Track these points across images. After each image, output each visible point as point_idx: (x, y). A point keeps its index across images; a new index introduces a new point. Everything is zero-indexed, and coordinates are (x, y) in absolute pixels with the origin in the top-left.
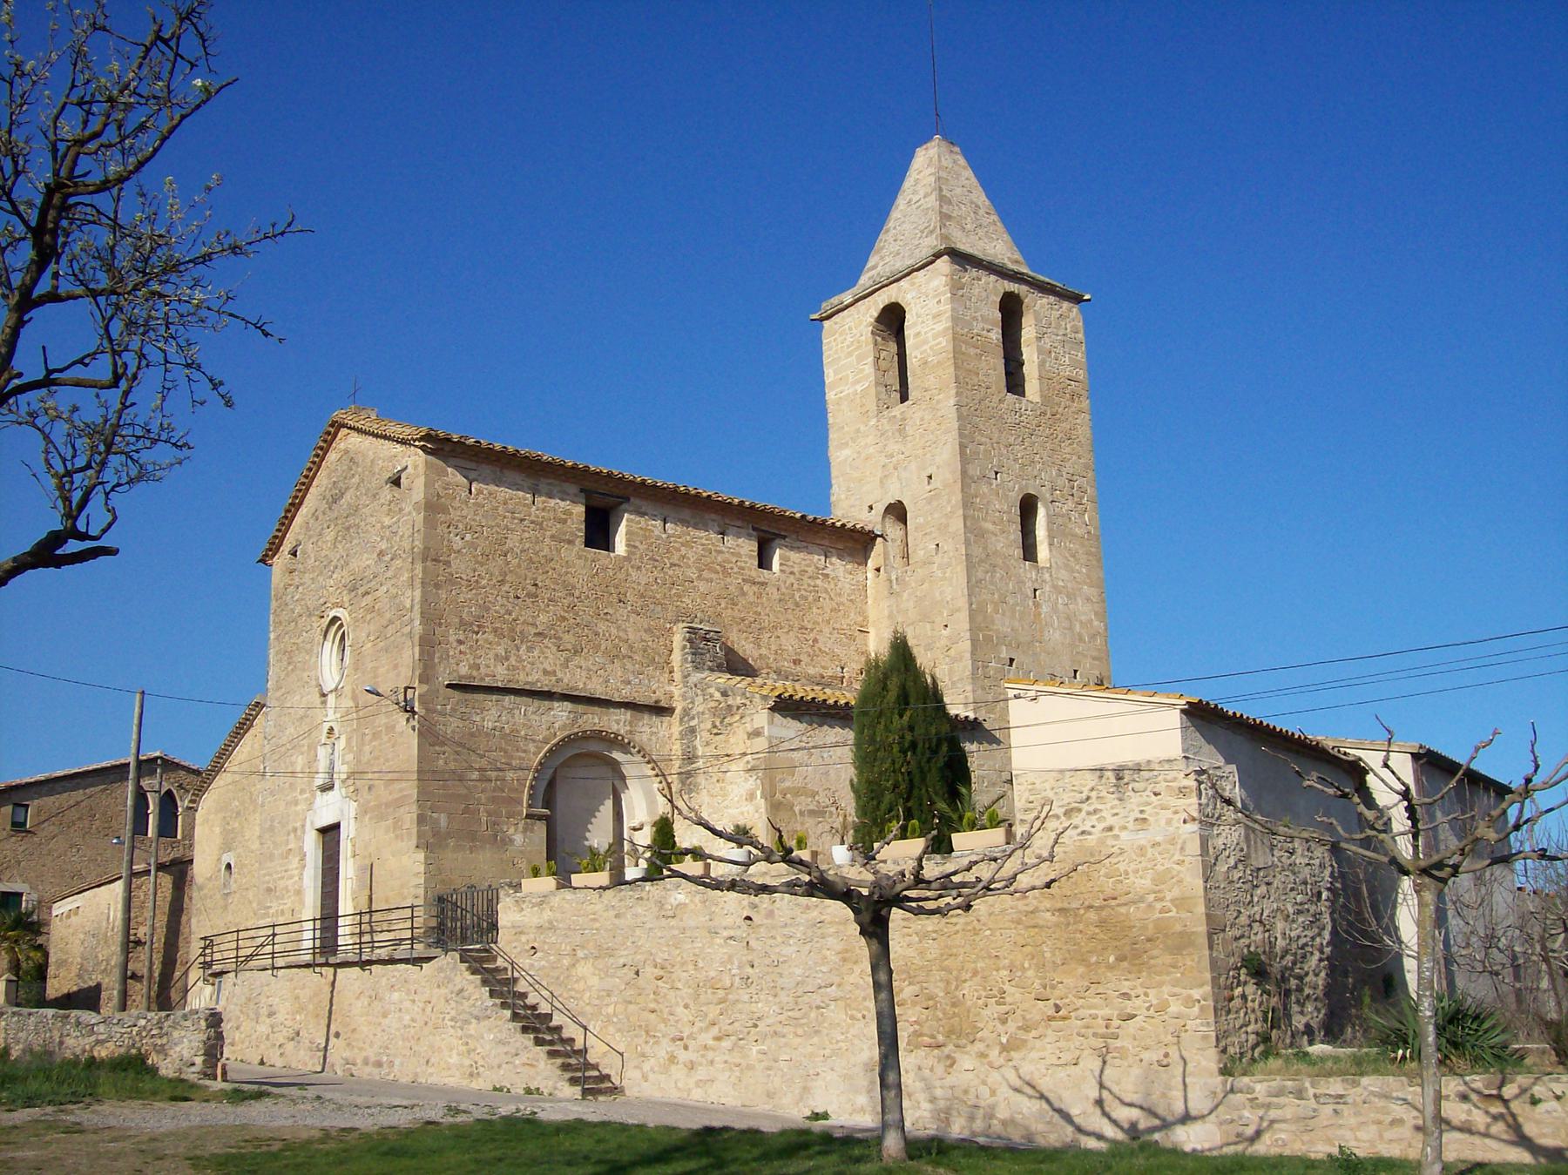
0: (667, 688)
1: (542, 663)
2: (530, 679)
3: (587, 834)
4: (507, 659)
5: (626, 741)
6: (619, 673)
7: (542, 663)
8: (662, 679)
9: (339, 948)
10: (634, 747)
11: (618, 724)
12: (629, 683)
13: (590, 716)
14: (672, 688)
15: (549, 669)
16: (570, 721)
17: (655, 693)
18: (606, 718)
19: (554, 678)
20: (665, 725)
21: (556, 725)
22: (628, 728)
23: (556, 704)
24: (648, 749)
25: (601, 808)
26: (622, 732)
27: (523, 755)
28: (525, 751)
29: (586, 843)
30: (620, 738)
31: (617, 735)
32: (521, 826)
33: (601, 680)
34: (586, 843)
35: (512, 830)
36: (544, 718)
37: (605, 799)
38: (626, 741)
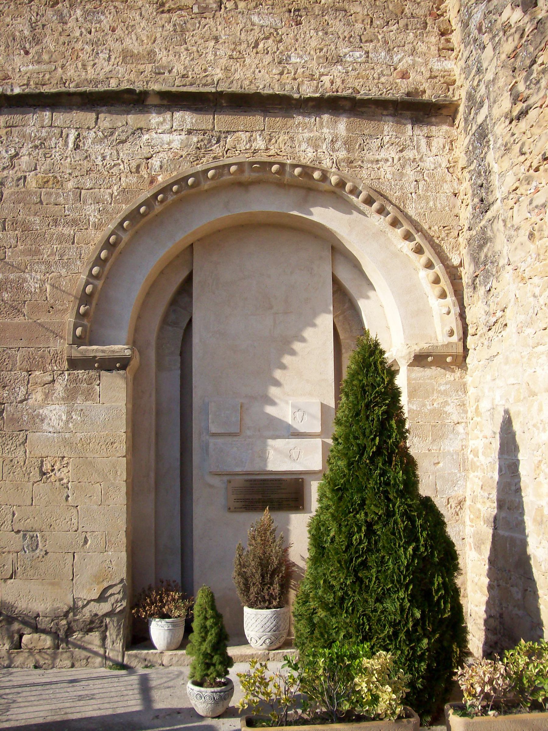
0: (437, 65)
1: (120, 40)
2: (91, 73)
3: (273, 391)
4: (37, 40)
5: (334, 179)
6: (314, 43)
7: (120, 40)
8: (422, 47)
9: (125, 662)
10: (355, 191)
11: (316, 147)
12: (339, 60)
13: (244, 136)
14: (449, 65)
15: (136, 48)
16: (192, 150)
17: (404, 75)
18: (283, 137)
19: (149, 67)
20: (437, 143)
21: (155, 162)
22: (342, 154)
23: (154, 119)
24: (395, 196)
25: (308, 333)
26: (327, 163)
27: (68, 231)
28: (75, 222)
29: (270, 410)
30: (316, 175)
31: (307, 171)
32: (59, 387)
33: (268, 59)
34: (270, 410)
35: (38, 396)
36: (125, 150)
37: (315, 315)
38: (334, 179)
